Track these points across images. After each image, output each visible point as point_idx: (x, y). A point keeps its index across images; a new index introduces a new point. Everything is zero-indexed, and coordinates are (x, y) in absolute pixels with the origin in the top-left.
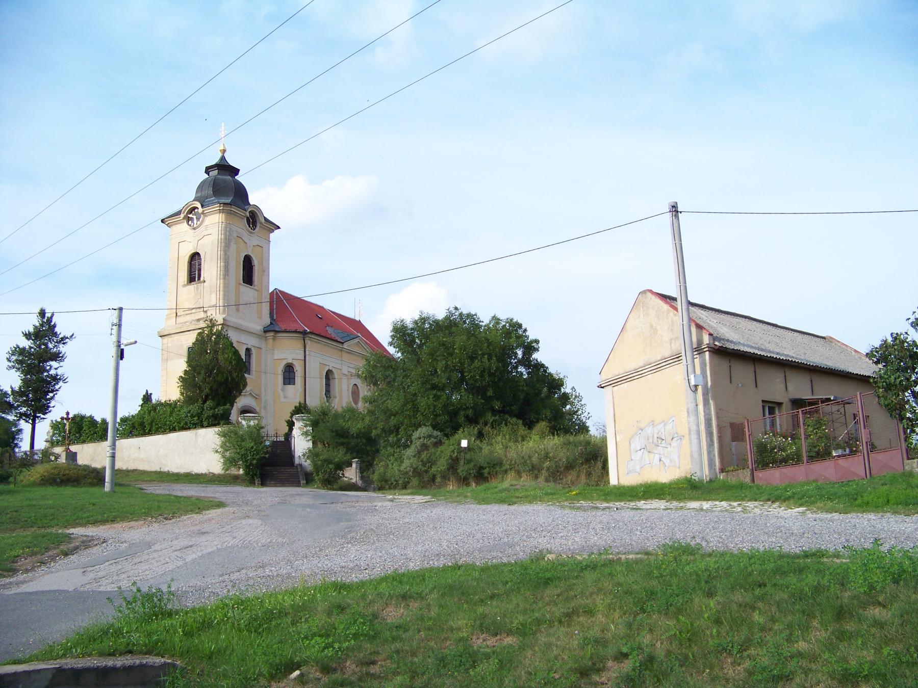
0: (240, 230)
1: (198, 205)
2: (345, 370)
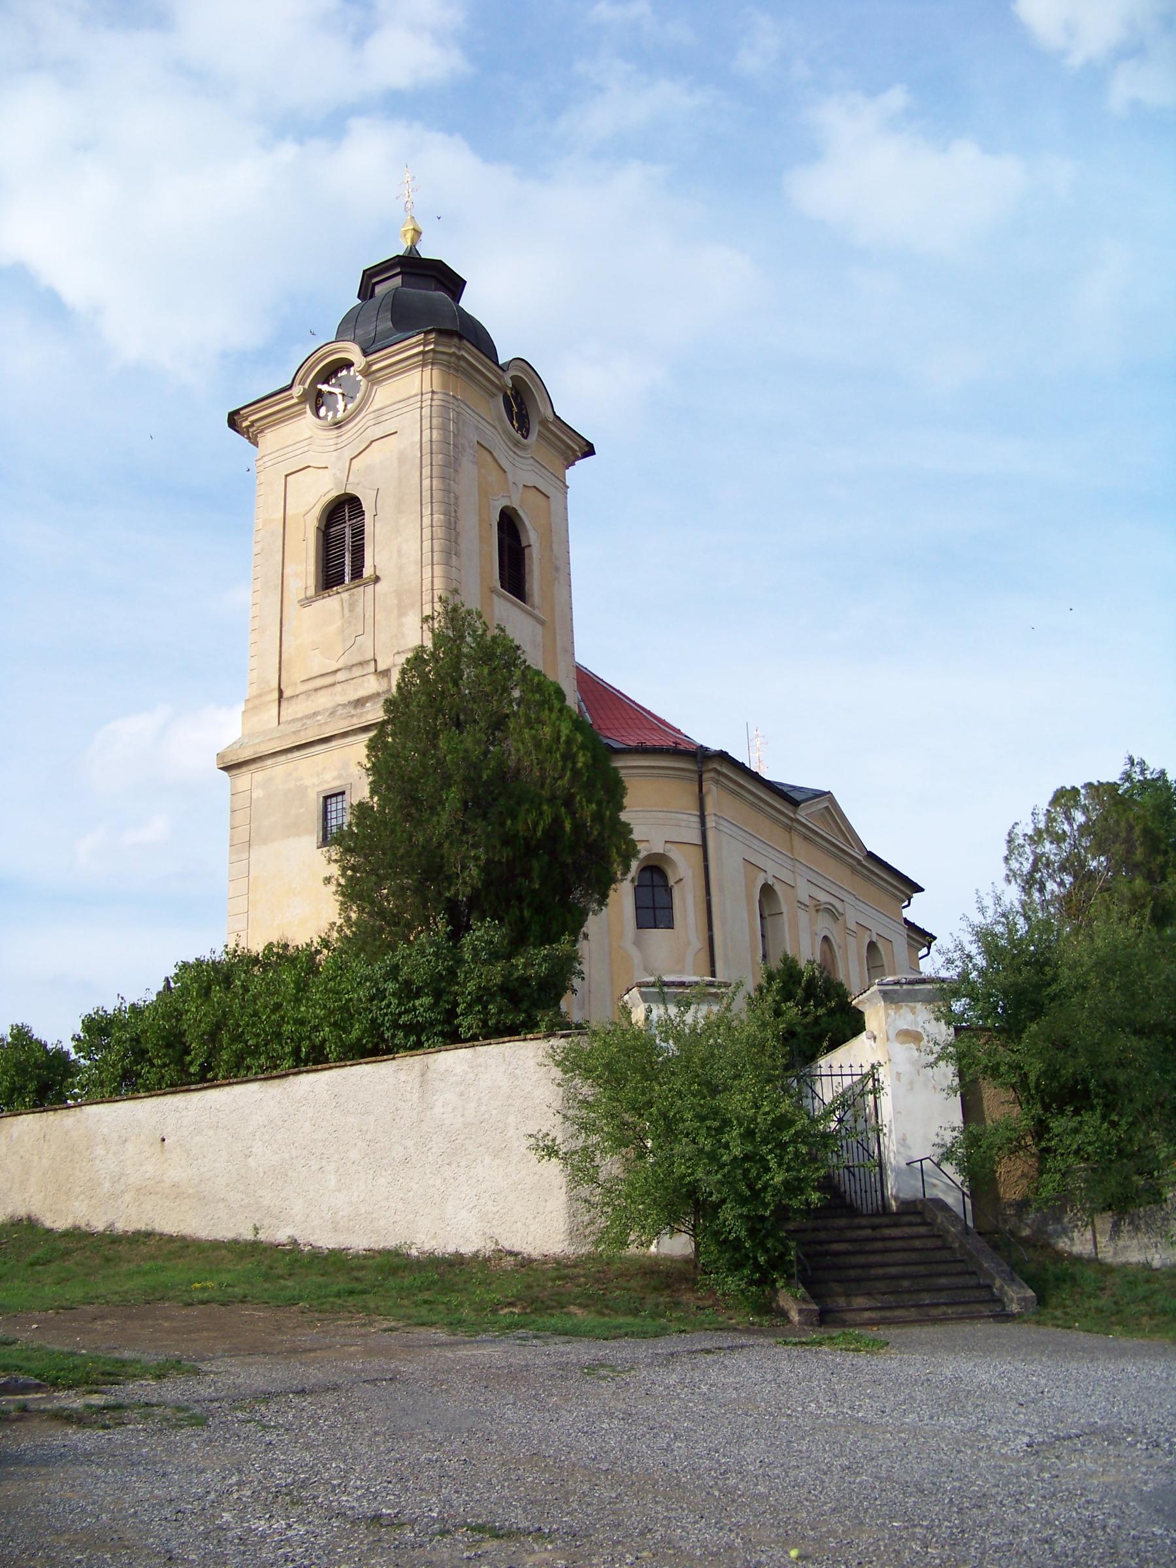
0: (489, 431)
1: (353, 352)
2: (804, 891)
